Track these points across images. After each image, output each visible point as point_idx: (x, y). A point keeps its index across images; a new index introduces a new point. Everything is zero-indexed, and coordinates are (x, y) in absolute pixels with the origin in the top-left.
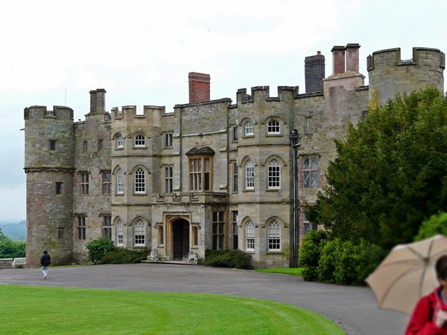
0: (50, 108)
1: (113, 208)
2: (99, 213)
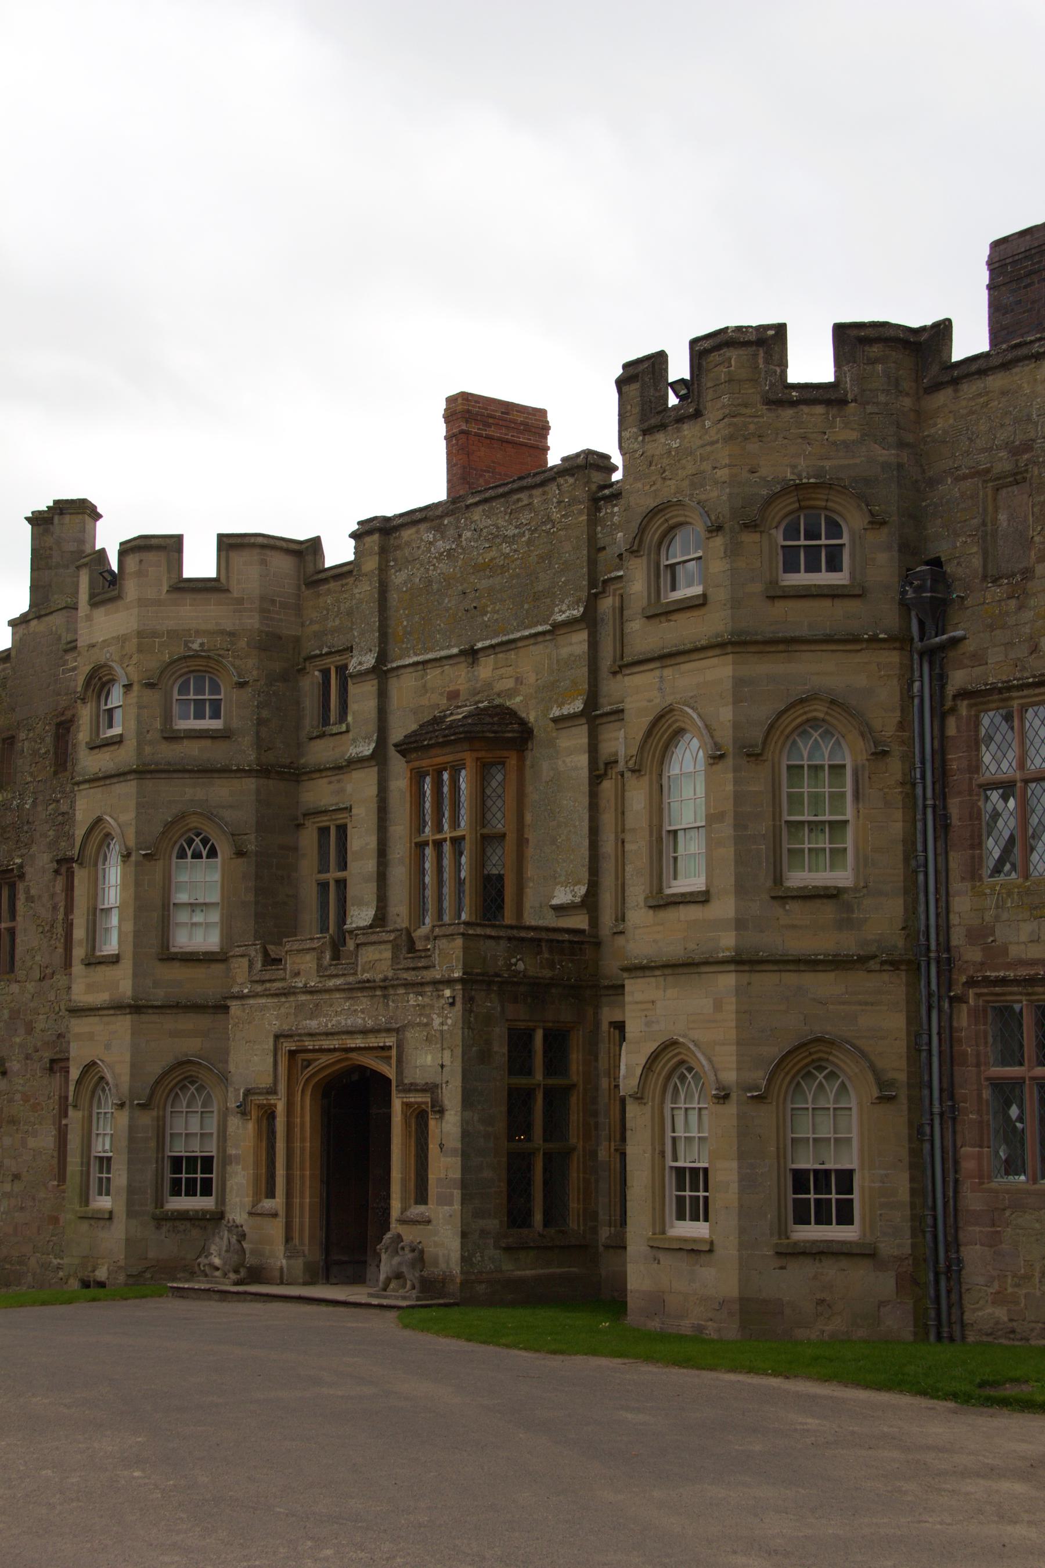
1: (79, 1026)
2: (47, 1055)
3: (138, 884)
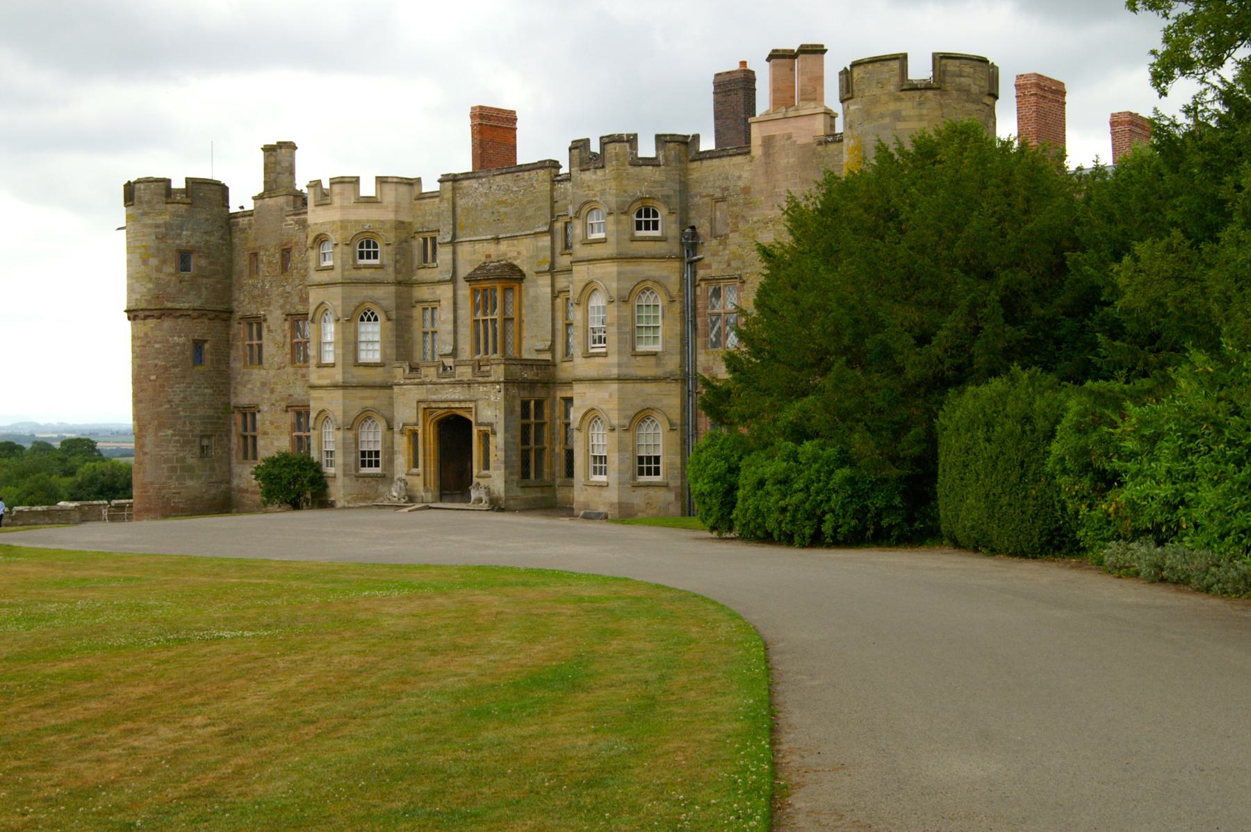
0: (178, 184)
1: (315, 393)
2: (284, 404)
3: (343, 333)
